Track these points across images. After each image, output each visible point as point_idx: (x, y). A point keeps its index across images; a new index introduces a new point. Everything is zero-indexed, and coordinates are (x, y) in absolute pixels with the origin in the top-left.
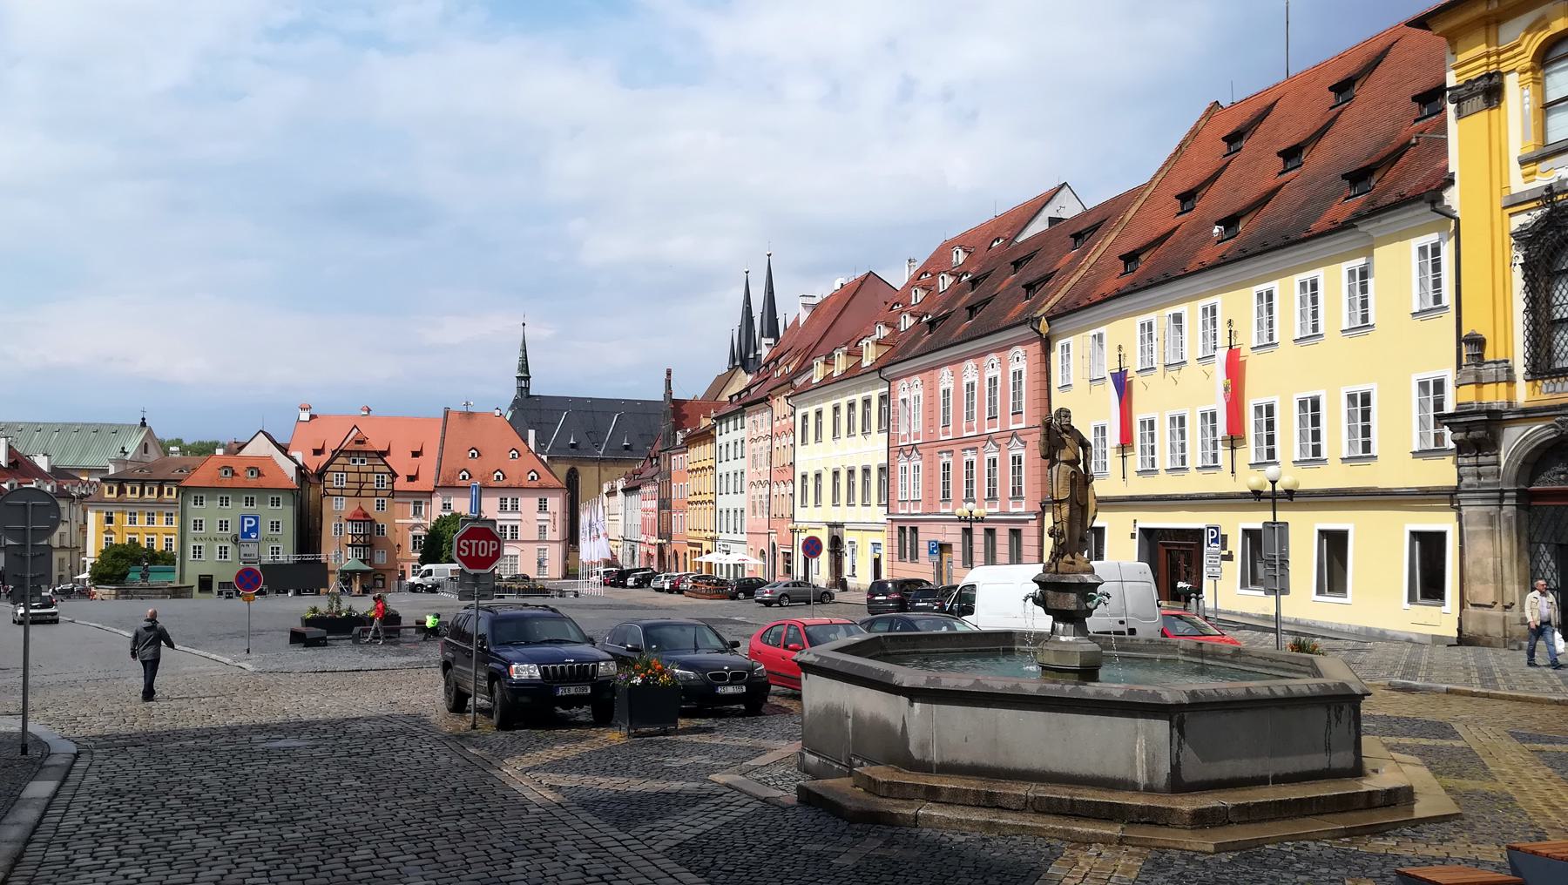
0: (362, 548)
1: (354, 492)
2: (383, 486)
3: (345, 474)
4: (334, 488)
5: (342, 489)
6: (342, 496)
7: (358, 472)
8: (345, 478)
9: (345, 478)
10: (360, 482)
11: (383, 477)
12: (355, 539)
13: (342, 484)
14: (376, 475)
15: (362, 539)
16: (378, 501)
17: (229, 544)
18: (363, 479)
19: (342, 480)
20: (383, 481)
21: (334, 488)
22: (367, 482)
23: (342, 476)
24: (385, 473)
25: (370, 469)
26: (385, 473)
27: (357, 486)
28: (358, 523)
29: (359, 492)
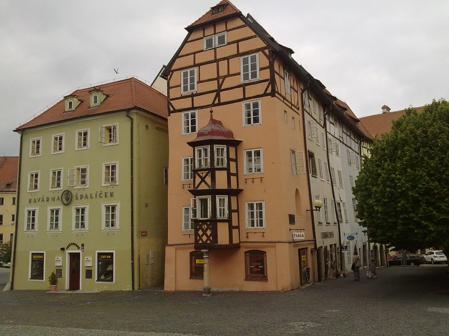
0: (209, 198)
1: (209, 99)
2: (254, 75)
3: (196, 69)
4: (182, 97)
5: (192, 96)
6: (193, 108)
7: (216, 61)
8: (196, 76)
9: (196, 76)
10: (217, 79)
11: (253, 59)
12: (198, 180)
13: (192, 87)
14: (242, 58)
15: (208, 180)
16: (248, 106)
17: (61, 207)
18: (224, 72)
19: (192, 80)
20: (254, 67)
21: (182, 97)
22: (229, 75)
23: (192, 73)
24: (257, 50)
25: (232, 50)
26: (257, 50)
27: (214, 86)
28: (201, 148)
29: (218, 96)
